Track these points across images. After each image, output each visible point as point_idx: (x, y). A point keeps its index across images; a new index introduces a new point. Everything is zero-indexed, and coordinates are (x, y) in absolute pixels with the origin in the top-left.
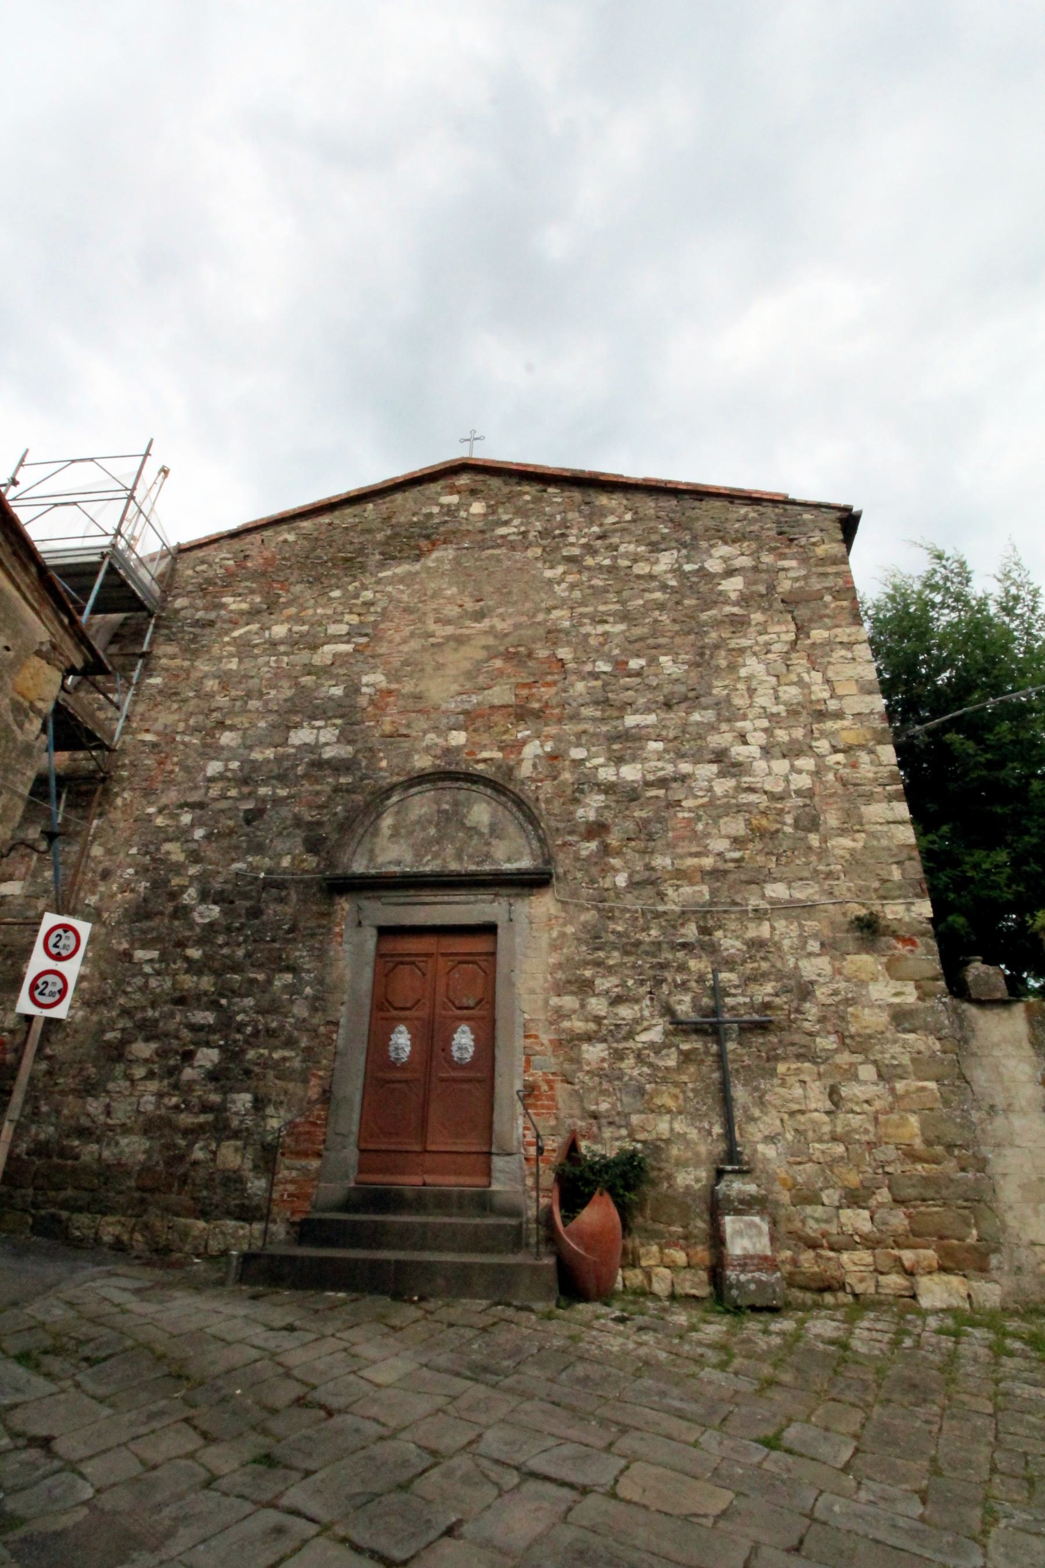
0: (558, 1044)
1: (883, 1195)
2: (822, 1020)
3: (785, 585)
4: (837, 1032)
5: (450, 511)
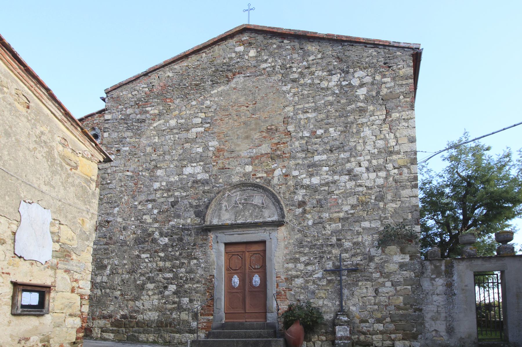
0: (287, 279)
1: (388, 320)
2: (376, 268)
3: (384, 91)
4: (380, 272)
5: (240, 56)
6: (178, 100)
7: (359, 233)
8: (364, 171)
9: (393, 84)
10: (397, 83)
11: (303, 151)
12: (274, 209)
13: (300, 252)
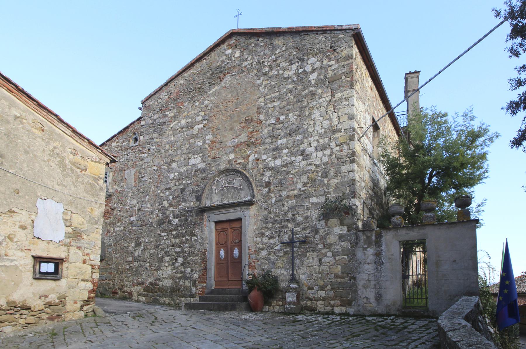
0: (256, 251)
1: (329, 287)
2: (320, 240)
3: (330, 74)
4: (323, 243)
5: (229, 58)
6: (187, 103)
7: (308, 208)
8: (313, 151)
9: (337, 66)
10: (340, 64)
11: (270, 136)
12: (248, 190)
13: (265, 228)
